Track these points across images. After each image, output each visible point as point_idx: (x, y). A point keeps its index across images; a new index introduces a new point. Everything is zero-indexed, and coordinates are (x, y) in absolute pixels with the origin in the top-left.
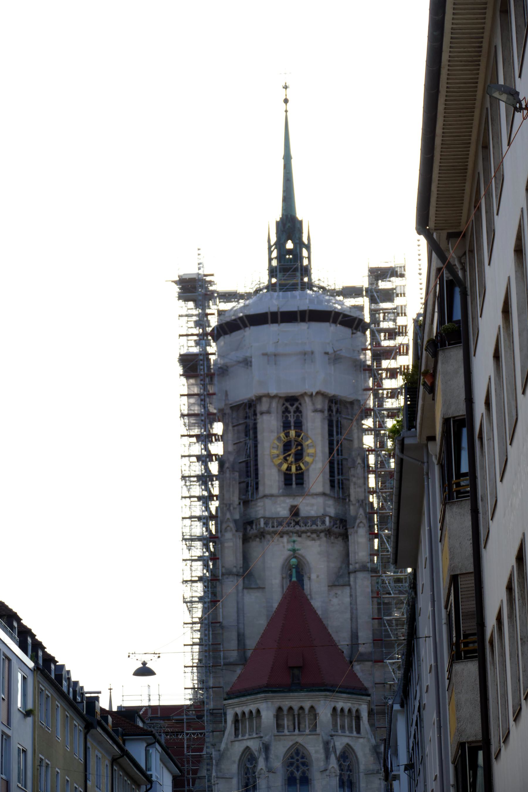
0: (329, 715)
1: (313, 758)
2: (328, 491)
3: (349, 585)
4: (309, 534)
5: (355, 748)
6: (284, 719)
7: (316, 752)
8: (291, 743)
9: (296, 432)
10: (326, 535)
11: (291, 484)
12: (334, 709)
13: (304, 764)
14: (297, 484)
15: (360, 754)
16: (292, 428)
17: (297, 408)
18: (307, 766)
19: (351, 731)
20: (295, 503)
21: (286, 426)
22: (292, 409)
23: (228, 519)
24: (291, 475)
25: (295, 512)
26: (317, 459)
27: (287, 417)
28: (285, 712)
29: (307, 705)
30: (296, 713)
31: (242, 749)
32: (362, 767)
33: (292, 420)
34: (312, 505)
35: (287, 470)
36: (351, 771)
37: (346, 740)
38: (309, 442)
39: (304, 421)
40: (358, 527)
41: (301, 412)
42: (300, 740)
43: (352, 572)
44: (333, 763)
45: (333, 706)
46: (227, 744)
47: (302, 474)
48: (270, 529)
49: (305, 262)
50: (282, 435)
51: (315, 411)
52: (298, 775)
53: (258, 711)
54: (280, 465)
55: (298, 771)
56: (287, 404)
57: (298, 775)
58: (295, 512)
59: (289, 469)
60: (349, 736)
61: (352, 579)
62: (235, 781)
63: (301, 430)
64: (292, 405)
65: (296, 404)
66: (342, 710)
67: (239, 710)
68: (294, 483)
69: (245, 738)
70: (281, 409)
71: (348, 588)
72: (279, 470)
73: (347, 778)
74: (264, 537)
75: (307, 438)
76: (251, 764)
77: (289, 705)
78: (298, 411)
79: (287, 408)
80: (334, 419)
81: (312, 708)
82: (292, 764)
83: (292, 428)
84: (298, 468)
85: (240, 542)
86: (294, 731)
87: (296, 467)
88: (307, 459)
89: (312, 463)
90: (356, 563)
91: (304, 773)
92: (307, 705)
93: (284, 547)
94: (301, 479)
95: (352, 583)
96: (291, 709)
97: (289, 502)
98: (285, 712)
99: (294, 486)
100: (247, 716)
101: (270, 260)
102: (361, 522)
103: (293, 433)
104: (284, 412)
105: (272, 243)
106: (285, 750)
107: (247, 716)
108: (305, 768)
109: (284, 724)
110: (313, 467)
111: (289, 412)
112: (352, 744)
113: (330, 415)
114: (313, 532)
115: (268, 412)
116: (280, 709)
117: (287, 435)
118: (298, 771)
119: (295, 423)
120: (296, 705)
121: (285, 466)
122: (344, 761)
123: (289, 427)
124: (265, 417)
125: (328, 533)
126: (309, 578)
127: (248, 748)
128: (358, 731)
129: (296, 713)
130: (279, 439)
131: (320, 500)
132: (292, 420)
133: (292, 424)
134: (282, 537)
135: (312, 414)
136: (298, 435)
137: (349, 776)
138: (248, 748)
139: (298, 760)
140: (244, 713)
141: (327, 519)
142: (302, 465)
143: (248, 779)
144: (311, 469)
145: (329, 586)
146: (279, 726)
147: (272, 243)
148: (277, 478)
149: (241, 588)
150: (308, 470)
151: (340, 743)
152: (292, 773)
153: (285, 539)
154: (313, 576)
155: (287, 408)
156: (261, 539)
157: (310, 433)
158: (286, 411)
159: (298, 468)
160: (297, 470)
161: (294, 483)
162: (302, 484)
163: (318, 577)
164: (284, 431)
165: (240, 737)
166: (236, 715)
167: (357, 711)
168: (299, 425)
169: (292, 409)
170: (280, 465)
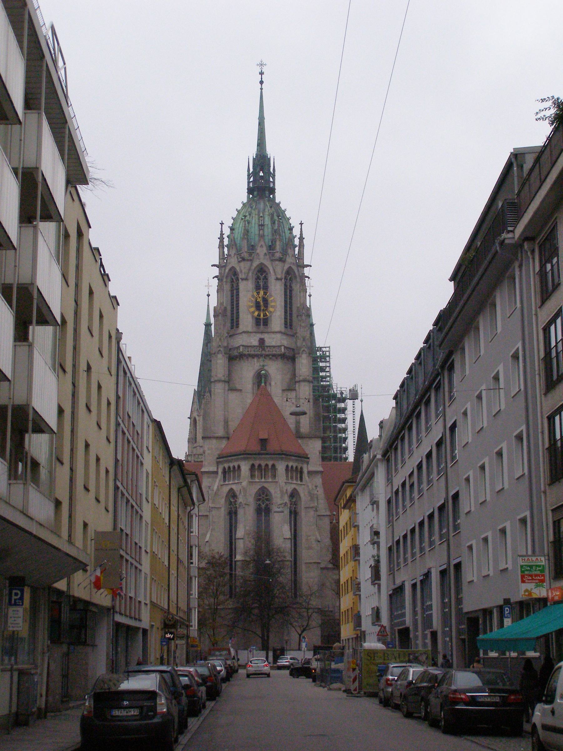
0: (284, 470)
1: (273, 496)
2: (283, 330)
3: (295, 390)
4: (270, 357)
5: (299, 491)
6: (255, 472)
7: (275, 492)
8: (259, 487)
9: (264, 292)
10: (282, 357)
11: (260, 325)
12: (287, 466)
13: (267, 500)
14: (264, 325)
15: (302, 495)
16: (262, 290)
17: (265, 277)
18: (269, 501)
19: (297, 479)
20: (262, 337)
21: (258, 288)
22: (262, 277)
23: (220, 345)
24: (260, 319)
25: (262, 341)
26: (277, 309)
27: (258, 282)
28: (256, 467)
29: (270, 463)
30: (263, 468)
31: (228, 490)
32: (303, 503)
33: (261, 284)
34: (274, 338)
36: (296, 505)
37: (293, 486)
38: (272, 298)
39: (269, 285)
40: (302, 353)
41: (267, 279)
42: (266, 485)
43: (297, 382)
44: (286, 499)
45: (286, 464)
46: (218, 486)
47: (267, 319)
48: (246, 352)
49: (271, 185)
50: (255, 294)
51: (277, 279)
52: (263, 506)
53: (239, 467)
54: (253, 312)
55: (263, 504)
56: (259, 274)
57: (263, 506)
58: (262, 341)
59: (259, 315)
60: (295, 484)
61: (297, 386)
62: (223, 509)
63: (267, 291)
64: (262, 275)
66: (292, 467)
67: (226, 466)
68: (262, 324)
69: (230, 483)
70: (255, 277)
71: (295, 391)
72: (253, 316)
73: (293, 509)
74: (242, 357)
75: (271, 296)
76: (234, 499)
77: (259, 463)
78: (266, 278)
80: (288, 284)
81: (273, 466)
82: (259, 500)
83: (262, 290)
84: (265, 315)
85: (227, 361)
86: (262, 478)
87: (264, 314)
88: (271, 309)
89: (274, 312)
90: (300, 376)
91: (267, 505)
92: (270, 463)
93: (255, 364)
95: (297, 388)
96: (260, 465)
97: (259, 336)
98: (256, 467)
99: (262, 326)
100: (232, 469)
101: (249, 182)
102: (304, 350)
103: (262, 292)
104: (256, 279)
105: (250, 172)
106: (256, 491)
107: (232, 469)
108: (267, 502)
109: (255, 475)
110: (274, 314)
112: (297, 488)
113: (285, 282)
114: (274, 355)
115: (246, 279)
116: (253, 465)
117: (258, 293)
118: (263, 504)
119: (263, 286)
120: (263, 464)
121: (256, 313)
122: (292, 499)
123: (260, 289)
124: (245, 282)
125: (283, 356)
126: (270, 384)
127: (231, 489)
128: (301, 480)
129: (263, 468)
130: (253, 296)
131: (279, 336)
132: (261, 284)
134: (253, 358)
135: (275, 281)
136: (265, 293)
137: (295, 508)
138: (231, 489)
139: (263, 497)
140: (229, 468)
141: (283, 348)
142: (267, 313)
143: (231, 508)
144: (273, 316)
145: (282, 390)
146: (252, 476)
147: (250, 172)
148: (251, 321)
149: (227, 388)
150: (271, 316)
151: (290, 488)
152: (260, 505)
153: (255, 360)
154: (273, 383)
156: (240, 359)
157: (273, 294)
158: (258, 278)
159: (265, 315)
160: (264, 316)
161: (262, 324)
162: (267, 325)
163: (276, 383)
164: (256, 291)
165: (227, 483)
166: (224, 468)
167: (301, 468)
168: (266, 288)
169: (262, 277)
170: (253, 312)
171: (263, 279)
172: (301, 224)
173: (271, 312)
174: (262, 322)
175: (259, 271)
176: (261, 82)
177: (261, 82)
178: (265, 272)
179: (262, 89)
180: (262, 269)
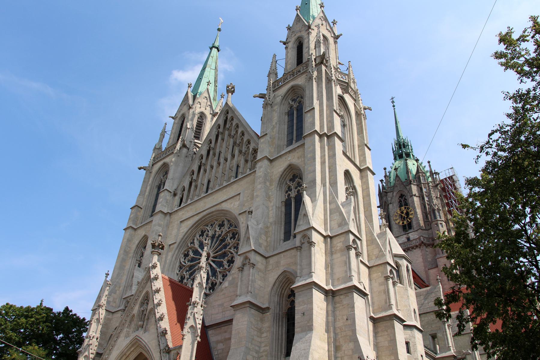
17: (405, 198)
21: (401, 206)
35: (402, 223)
54: (399, 223)
56: (401, 199)
59: (403, 223)
65: (404, 197)
79: (400, 200)
88: (410, 216)
94: (410, 226)
104: (399, 202)
111: (402, 201)
133: (403, 204)
142: (408, 220)
155: (400, 200)
158: (400, 201)
171: (404, 201)
172: (429, 162)
173: (411, 218)
174: (407, 227)
175: (400, 197)
176: (394, 106)
177: (394, 106)
178: (404, 195)
179: (394, 109)
180: (402, 195)
